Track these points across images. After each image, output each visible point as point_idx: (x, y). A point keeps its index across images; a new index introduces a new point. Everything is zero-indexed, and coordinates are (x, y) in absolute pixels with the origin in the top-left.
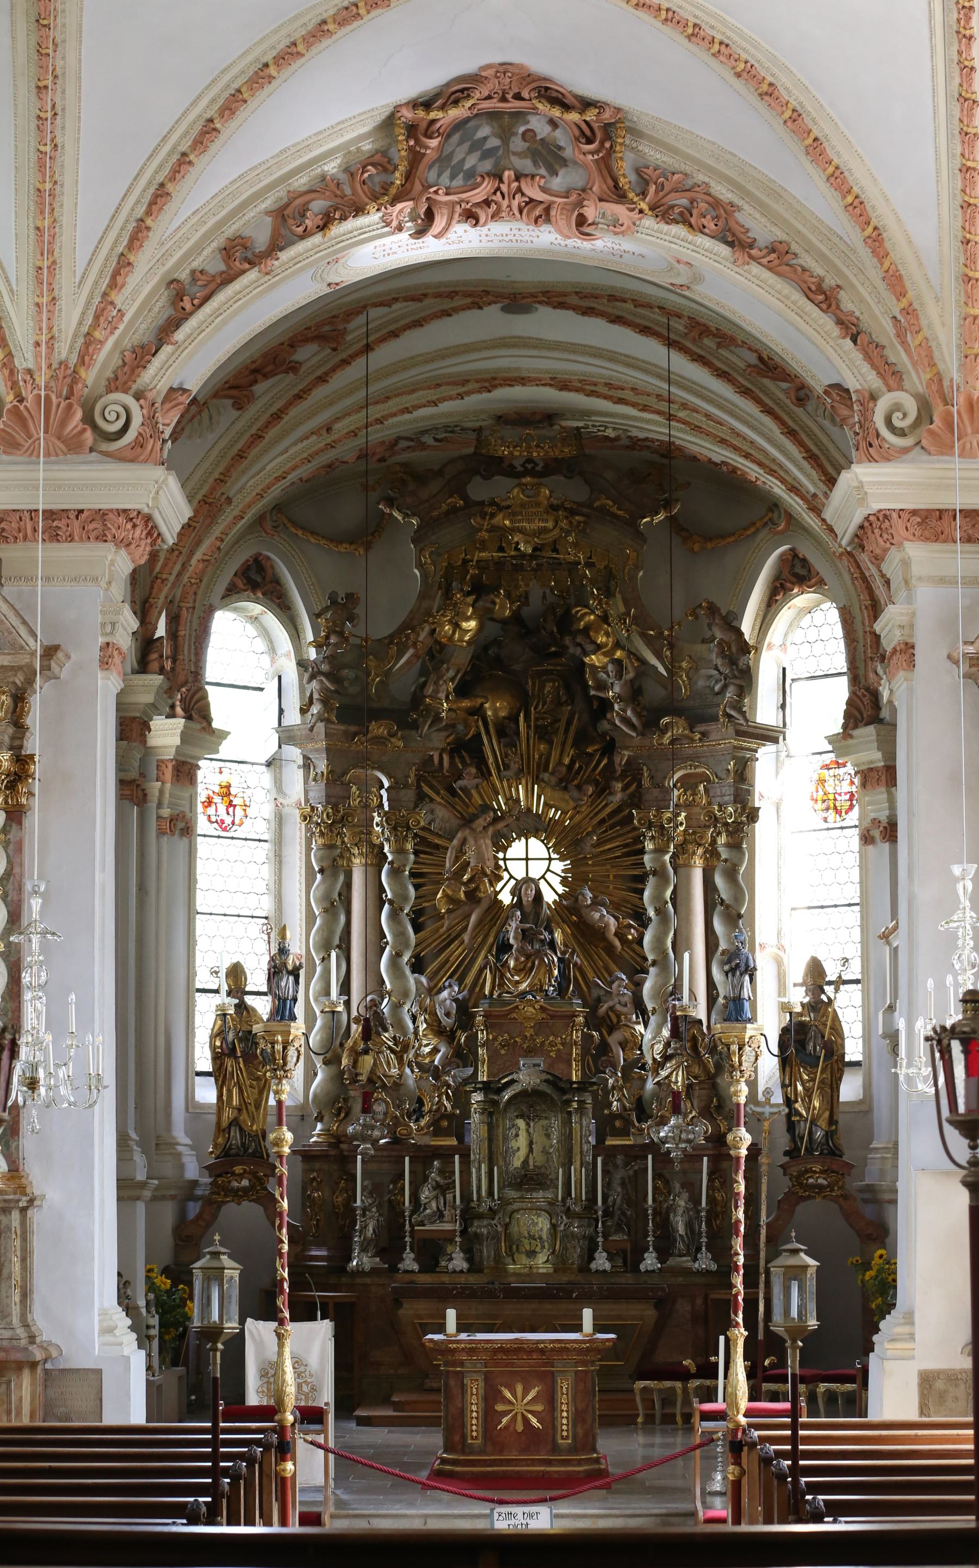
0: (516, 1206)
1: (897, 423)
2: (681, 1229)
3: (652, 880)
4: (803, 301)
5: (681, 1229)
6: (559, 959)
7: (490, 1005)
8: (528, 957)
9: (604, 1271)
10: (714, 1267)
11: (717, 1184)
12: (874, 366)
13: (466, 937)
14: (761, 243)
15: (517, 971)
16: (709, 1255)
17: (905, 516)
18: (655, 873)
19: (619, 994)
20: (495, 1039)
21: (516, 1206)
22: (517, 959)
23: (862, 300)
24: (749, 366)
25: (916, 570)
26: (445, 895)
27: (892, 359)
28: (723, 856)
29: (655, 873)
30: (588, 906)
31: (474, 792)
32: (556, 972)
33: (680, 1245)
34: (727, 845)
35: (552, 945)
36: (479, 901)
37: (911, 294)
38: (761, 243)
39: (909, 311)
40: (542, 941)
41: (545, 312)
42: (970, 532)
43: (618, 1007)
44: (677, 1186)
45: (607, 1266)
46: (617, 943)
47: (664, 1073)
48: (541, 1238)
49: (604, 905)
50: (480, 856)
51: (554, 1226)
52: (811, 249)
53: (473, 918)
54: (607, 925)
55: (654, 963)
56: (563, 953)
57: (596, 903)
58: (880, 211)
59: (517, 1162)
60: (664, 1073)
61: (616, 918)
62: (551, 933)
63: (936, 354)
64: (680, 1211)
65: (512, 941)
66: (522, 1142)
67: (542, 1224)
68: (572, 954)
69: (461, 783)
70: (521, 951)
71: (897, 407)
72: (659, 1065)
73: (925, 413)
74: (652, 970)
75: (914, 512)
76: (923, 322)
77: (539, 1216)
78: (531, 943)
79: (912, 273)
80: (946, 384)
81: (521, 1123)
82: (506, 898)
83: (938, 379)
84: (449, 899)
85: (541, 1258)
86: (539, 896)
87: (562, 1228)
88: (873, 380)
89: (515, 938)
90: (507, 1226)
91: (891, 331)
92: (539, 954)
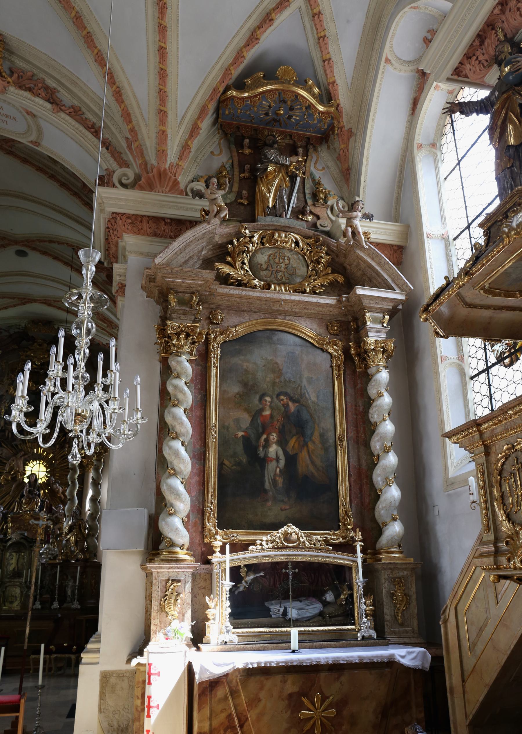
0: (8, 584)
1: (124, 181)
2: (69, 593)
3: (71, 472)
4: (84, 131)
5: (69, 593)
6: (41, 500)
7: (14, 514)
8: (30, 499)
9: (38, 609)
10: (79, 607)
11: (84, 576)
12: (115, 160)
13: (11, 493)
14: (67, 105)
15: (25, 504)
16: (78, 603)
17: (124, 219)
18: (72, 469)
19: (59, 512)
20: (14, 526)
21: (8, 584)
22: (25, 500)
23: (113, 133)
24: (104, 281)
25: (128, 248)
26: (4, 478)
27: (125, 158)
28: (95, 464)
29: (72, 469)
30: (53, 483)
31: (19, 446)
32: (39, 504)
33: (69, 599)
34: (96, 460)
35: (39, 495)
36: (16, 481)
37: (134, 122)
38: (67, 105)
39: (132, 130)
40: (36, 494)
41: (33, 256)
42: (156, 230)
43: (59, 516)
44: (69, 577)
45: (40, 607)
46: (62, 496)
47: (68, 537)
48: (16, 597)
49: (58, 483)
50: (18, 467)
51: (22, 592)
52: (90, 110)
53: (14, 486)
54: (59, 490)
55: (69, 500)
56: (43, 498)
57: (56, 482)
58: (121, 78)
59: (11, 568)
60: (68, 537)
61: (62, 488)
62: (39, 491)
63: (145, 152)
64: (70, 586)
65: (24, 493)
66: (14, 561)
67: (18, 591)
68: (46, 499)
69: (15, 443)
70: (28, 497)
71: (125, 175)
72: (67, 534)
73: (138, 178)
74: (69, 502)
75: (129, 216)
76: (140, 137)
77: (16, 588)
78: (32, 495)
79: (135, 113)
80: (149, 166)
81: (14, 554)
82: (26, 480)
83: (145, 164)
84: (6, 480)
85: (16, 604)
86: (36, 480)
87: (25, 593)
88: (114, 165)
89: (26, 492)
90: (4, 592)
91: (124, 145)
92: (34, 498)
